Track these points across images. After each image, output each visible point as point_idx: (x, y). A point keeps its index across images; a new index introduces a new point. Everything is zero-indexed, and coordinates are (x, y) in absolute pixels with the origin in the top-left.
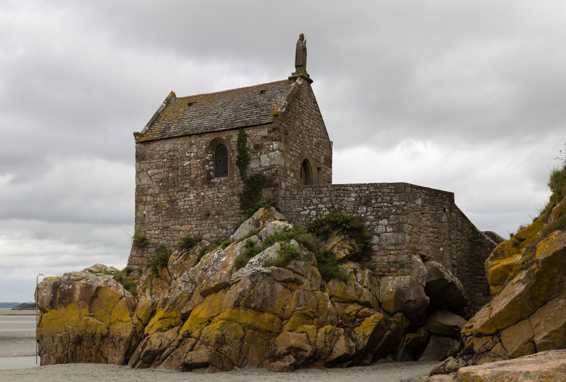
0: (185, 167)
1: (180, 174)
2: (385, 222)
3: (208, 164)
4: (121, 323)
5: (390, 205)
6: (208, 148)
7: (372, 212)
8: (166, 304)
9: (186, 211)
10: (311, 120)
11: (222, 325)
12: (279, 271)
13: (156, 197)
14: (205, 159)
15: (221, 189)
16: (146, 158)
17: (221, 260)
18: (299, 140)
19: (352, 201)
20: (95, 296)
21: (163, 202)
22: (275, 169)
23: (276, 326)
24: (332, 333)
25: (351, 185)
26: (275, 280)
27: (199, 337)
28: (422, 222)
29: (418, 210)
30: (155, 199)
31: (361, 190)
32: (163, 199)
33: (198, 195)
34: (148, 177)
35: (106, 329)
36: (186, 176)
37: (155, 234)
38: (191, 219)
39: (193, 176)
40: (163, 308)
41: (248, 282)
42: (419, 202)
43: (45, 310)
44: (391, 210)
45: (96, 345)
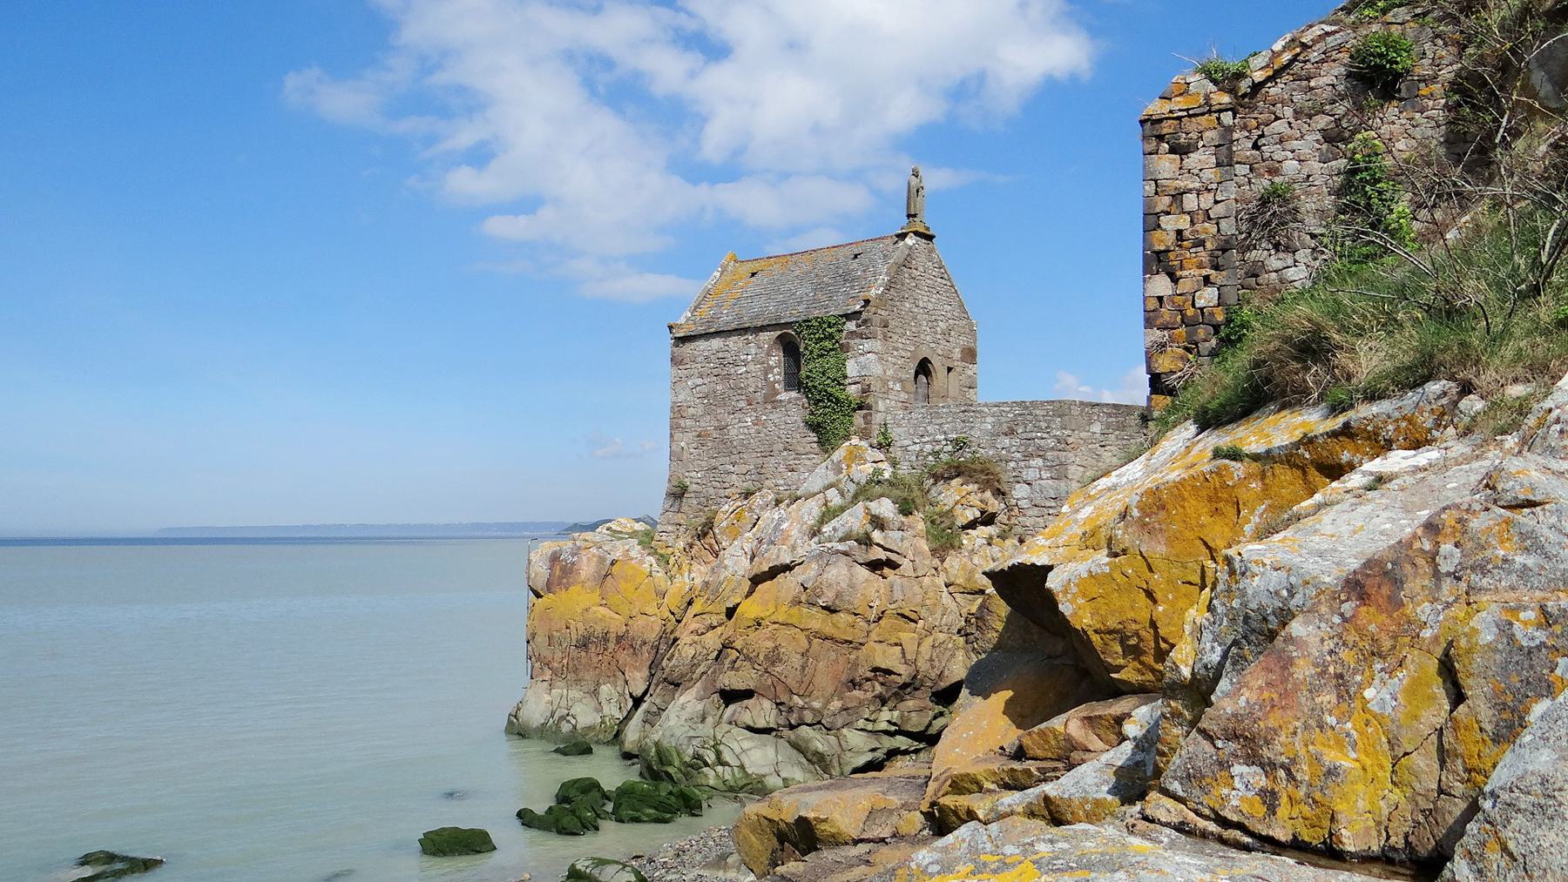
2: (1039, 462)
3: (772, 373)
5: (1045, 435)
10: (934, 296)
14: (768, 364)
18: (910, 330)
25: (986, 405)
28: (1102, 460)
29: (1094, 441)
39: (751, 390)
42: (1097, 428)
43: (538, 593)
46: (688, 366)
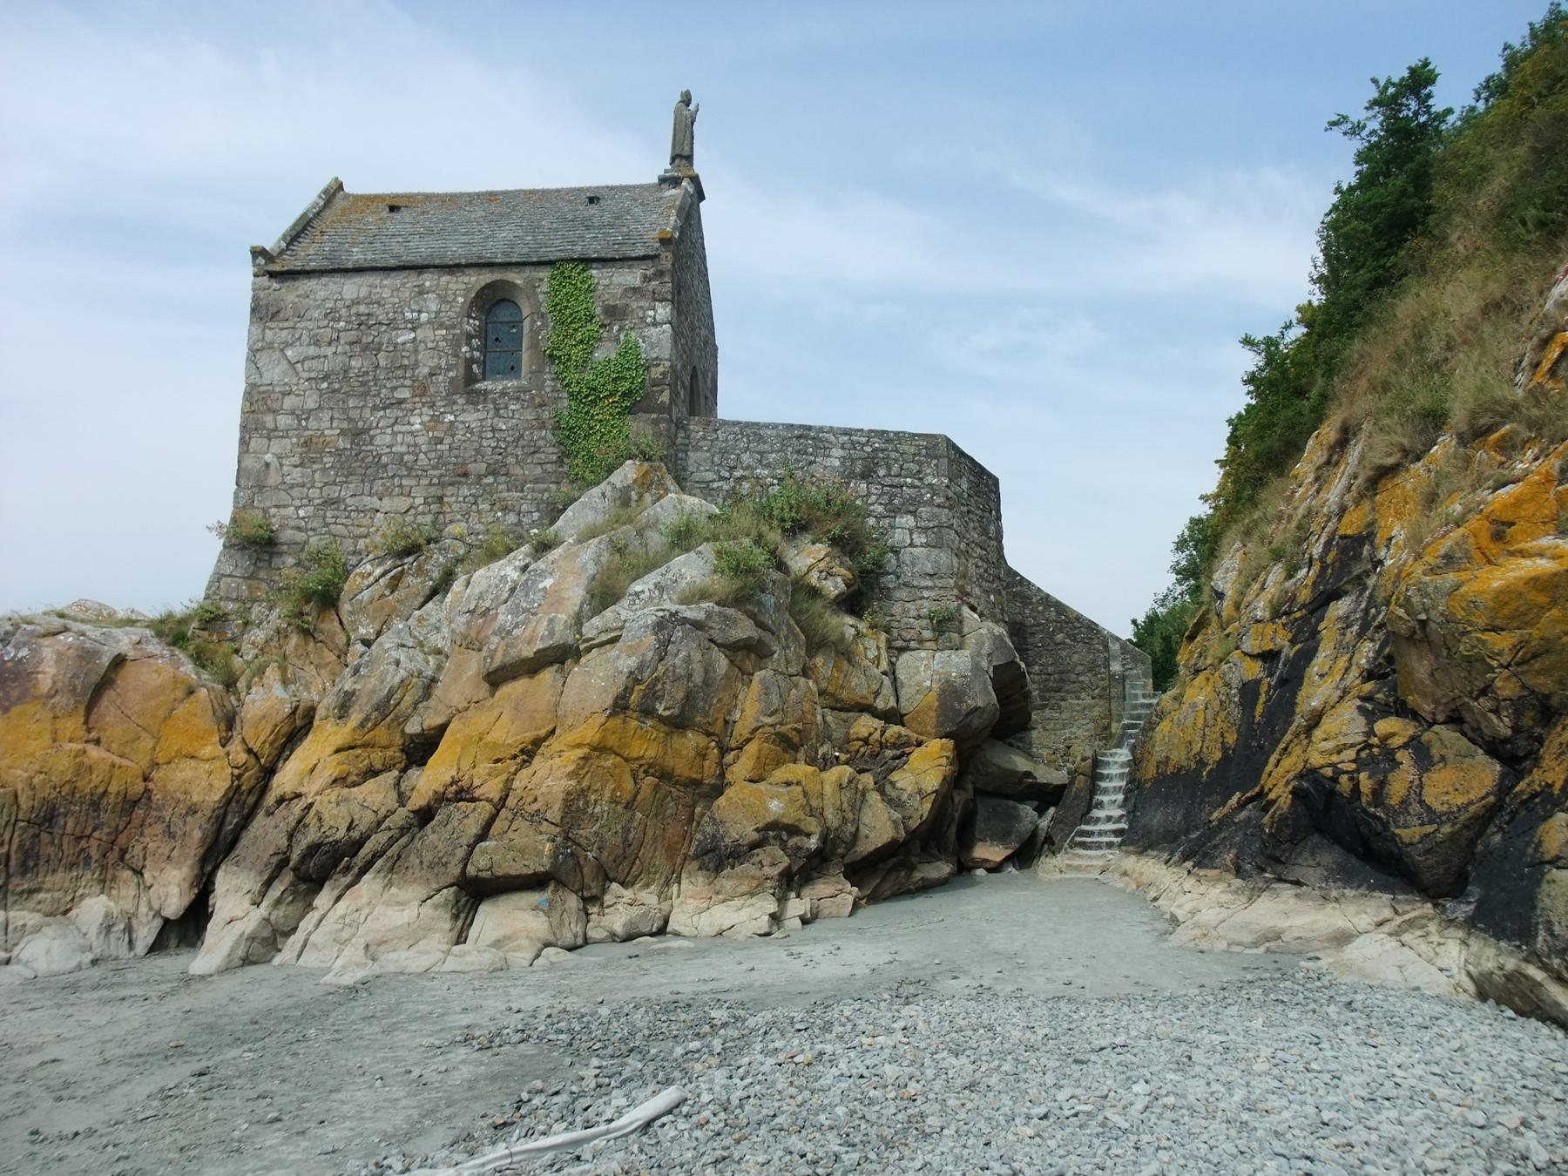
0: (400, 347)
1: (382, 363)
2: (909, 521)
4: (192, 763)
5: (917, 483)
6: (472, 303)
7: (880, 496)
8: (349, 707)
9: (399, 459)
11: (582, 762)
12: (726, 617)
13: (307, 419)
15: (506, 408)
16: (281, 315)
17: (541, 586)
19: (834, 468)
20: (105, 683)
21: (326, 432)
22: (661, 369)
23: (710, 765)
24: (853, 785)
25: (831, 430)
26: (711, 640)
27: (504, 799)
30: (304, 423)
31: (853, 443)
32: (328, 424)
33: (436, 419)
34: (284, 365)
35: (141, 779)
36: (398, 368)
37: (298, 518)
38: (413, 482)
39: (426, 370)
40: (340, 718)
41: (651, 640)
44: (923, 495)
45: (106, 830)
46: (286, 324)
